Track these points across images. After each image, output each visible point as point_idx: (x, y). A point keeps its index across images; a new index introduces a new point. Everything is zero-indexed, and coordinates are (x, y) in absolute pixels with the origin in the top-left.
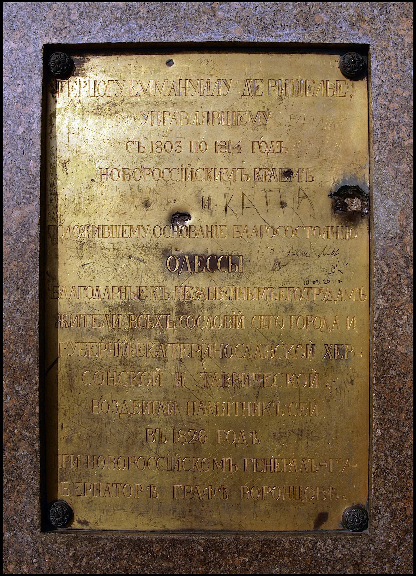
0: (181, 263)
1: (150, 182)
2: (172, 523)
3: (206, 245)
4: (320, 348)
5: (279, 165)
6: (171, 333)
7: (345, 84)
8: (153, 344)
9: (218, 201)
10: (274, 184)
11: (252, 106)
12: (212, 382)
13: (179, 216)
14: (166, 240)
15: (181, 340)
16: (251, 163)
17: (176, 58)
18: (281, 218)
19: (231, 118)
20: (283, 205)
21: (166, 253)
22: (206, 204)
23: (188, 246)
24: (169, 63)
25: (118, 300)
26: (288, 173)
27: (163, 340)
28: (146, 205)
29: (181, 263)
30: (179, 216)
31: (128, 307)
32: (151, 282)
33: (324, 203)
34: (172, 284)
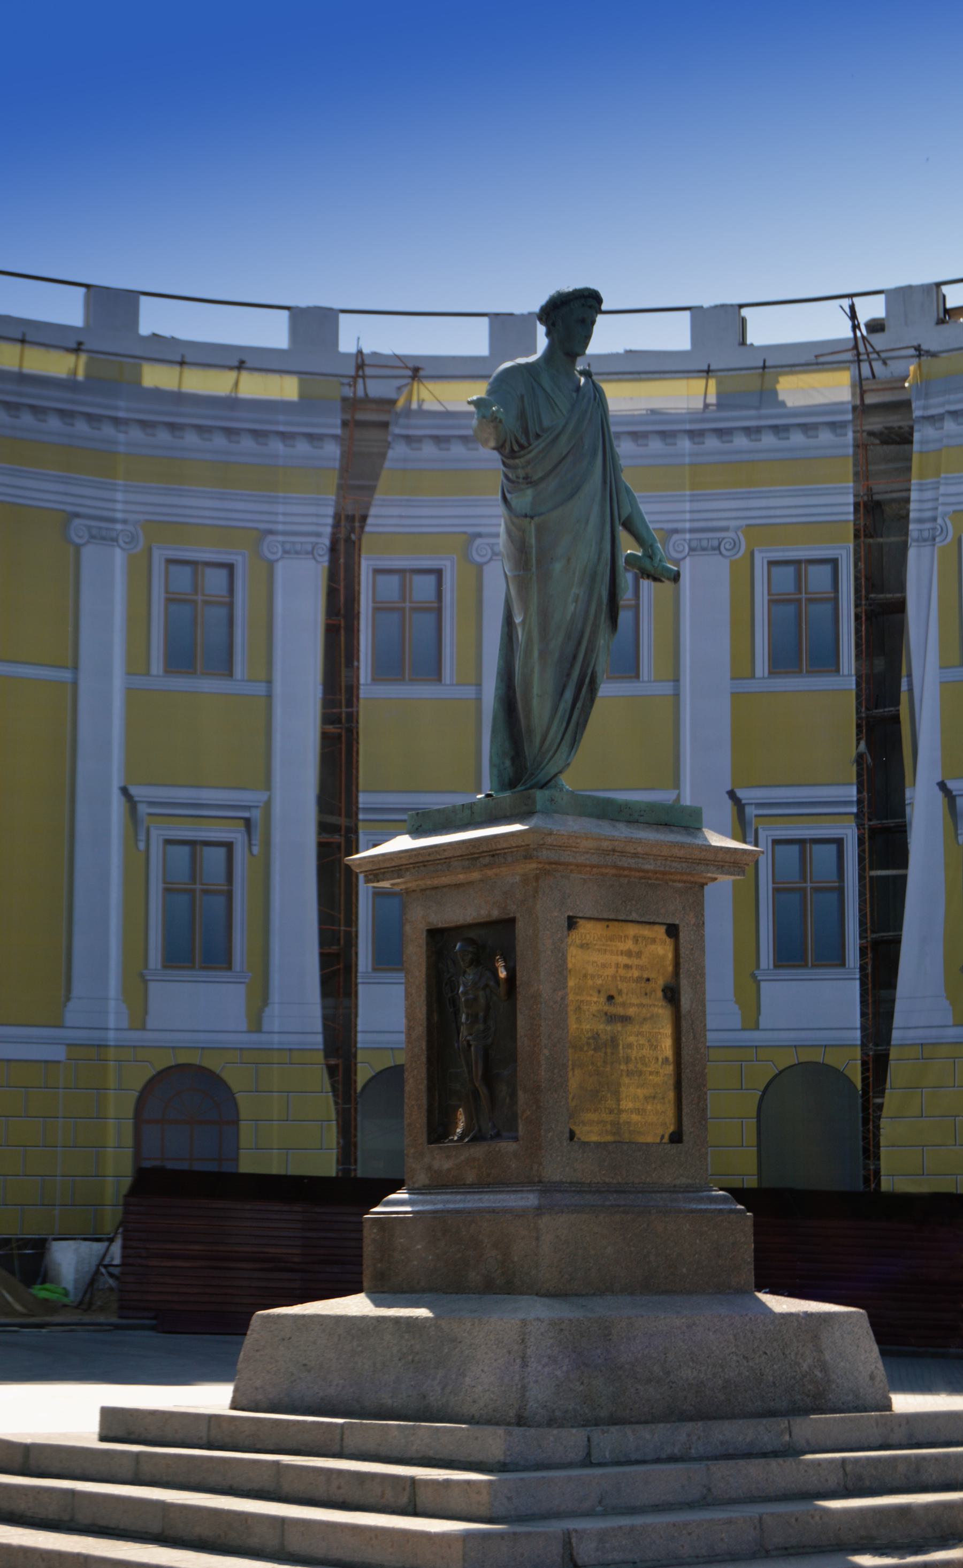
0: (611, 1019)
1: (599, 982)
2: (610, 1138)
3: (621, 1011)
4: (660, 1060)
5: (645, 976)
6: (609, 1051)
7: (668, 940)
8: (602, 1055)
9: (625, 991)
10: (643, 985)
11: (635, 948)
12: (624, 1073)
14: (606, 1008)
15: (612, 1054)
16: (636, 974)
17: (610, 924)
18: (645, 1001)
19: (629, 954)
20: (646, 994)
21: (606, 1014)
22: (620, 992)
23: (613, 1010)
24: (608, 926)
25: (590, 1034)
26: (648, 980)
27: (606, 1053)
28: (599, 992)
29: (611, 1019)
30: (611, 998)
32: (602, 1027)
33: (660, 994)
34: (609, 1028)
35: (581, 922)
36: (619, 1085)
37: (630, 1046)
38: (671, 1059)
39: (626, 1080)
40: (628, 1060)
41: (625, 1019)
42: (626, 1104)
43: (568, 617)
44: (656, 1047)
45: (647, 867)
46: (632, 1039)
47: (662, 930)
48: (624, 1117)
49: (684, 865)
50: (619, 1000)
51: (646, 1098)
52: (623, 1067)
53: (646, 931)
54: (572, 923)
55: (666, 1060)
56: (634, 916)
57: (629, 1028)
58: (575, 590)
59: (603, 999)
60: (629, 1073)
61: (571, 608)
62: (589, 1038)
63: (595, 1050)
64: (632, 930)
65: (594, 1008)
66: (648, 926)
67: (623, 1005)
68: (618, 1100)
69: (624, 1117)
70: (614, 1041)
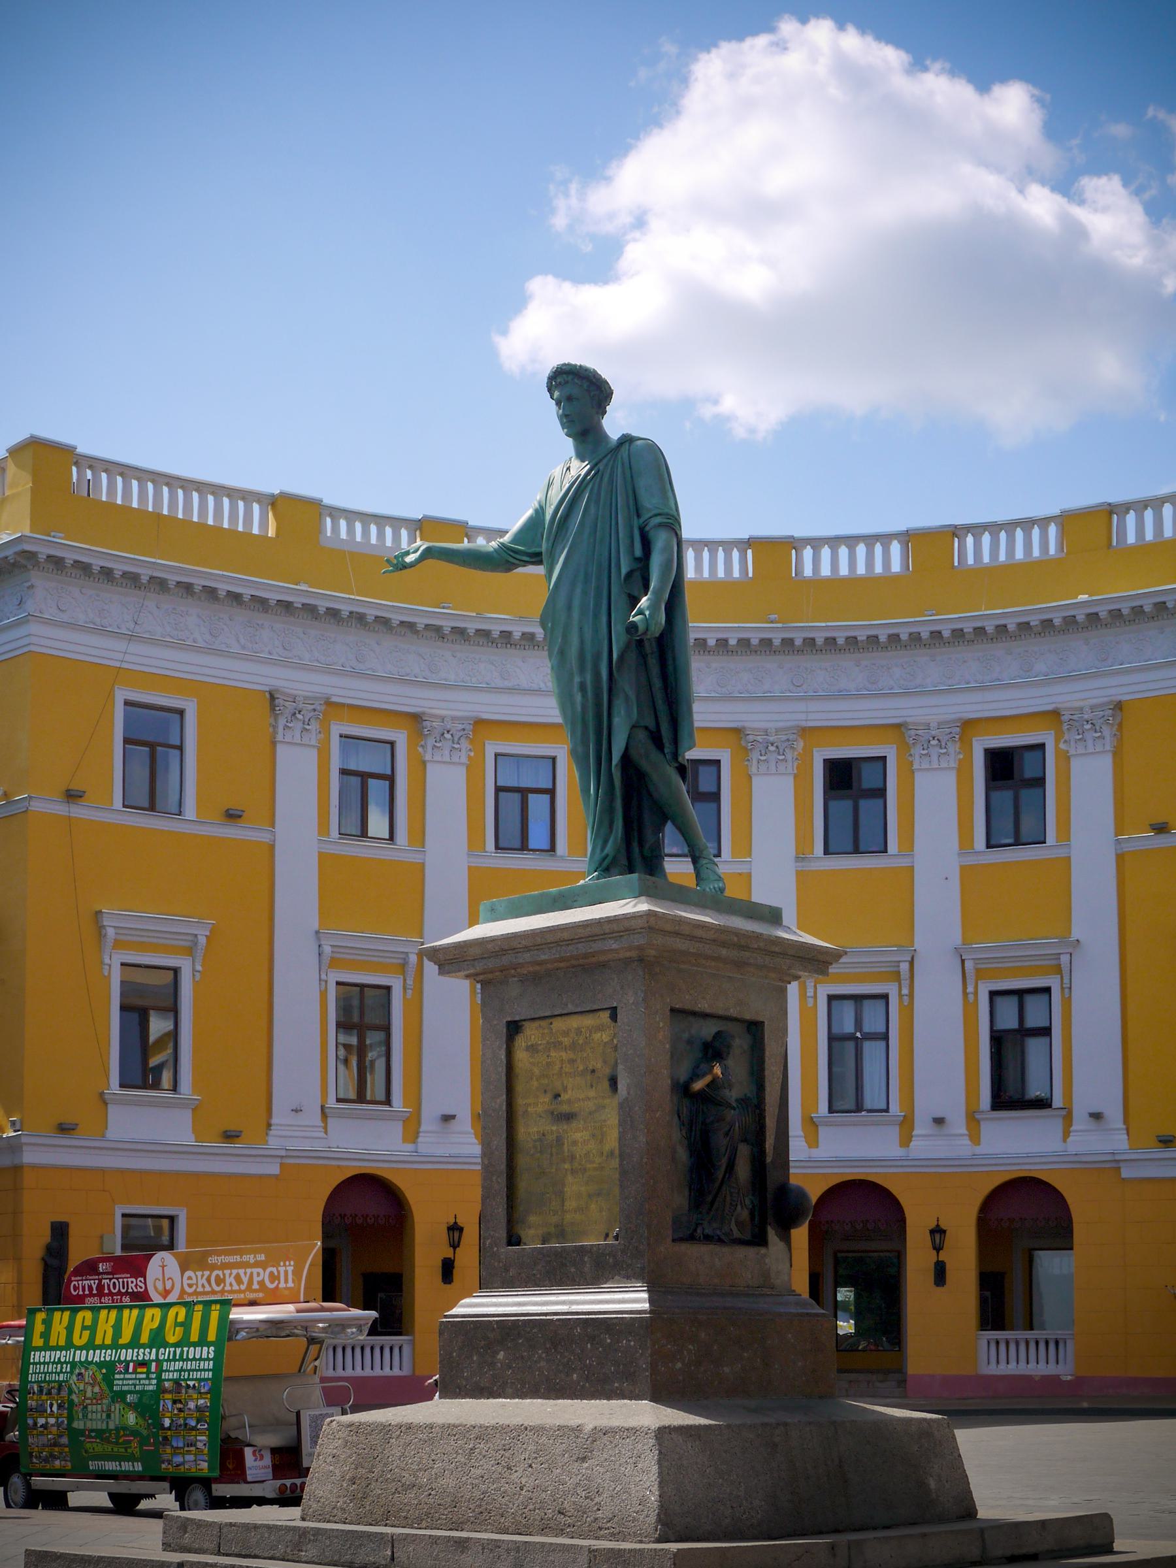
3: (565, 1108)
13: (557, 1096)
16: (581, 1068)
18: (592, 1093)
26: (593, 1071)
27: (552, 1155)
31: (540, 1140)
34: (554, 1128)
35: (526, 1024)
36: (564, 1185)
37: (575, 1143)
38: (617, 1152)
39: (570, 1179)
40: (573, 1158)
41: (568, 1117)
42: (571, 1204)
43: (579, 708)
44: (601, 1142)
45: (543, 957)
46: (578, 1136)
47: (605, 1016)
48: (568, 1217)
49: (580, 946)
50: (565, 1097)
51: (590, 1196)
52: (567, 1166)
53: (588, 1021)
54: (514, 1028)
55: (612, 1153)
56: (571, 1008)
57: (574, 1124)
58: (577, 679)
59: (547, 1099)
60: (573, 1172)
61: (578, 698)
62: (535, 1141)
63: (541, 1152)
64: (574, 1022)
65: (540, 1109)
66: (591, 1015)
67: (569, 1101)
68: (563, 1201)
69: (568, 1217)
70: (559, 1140)
